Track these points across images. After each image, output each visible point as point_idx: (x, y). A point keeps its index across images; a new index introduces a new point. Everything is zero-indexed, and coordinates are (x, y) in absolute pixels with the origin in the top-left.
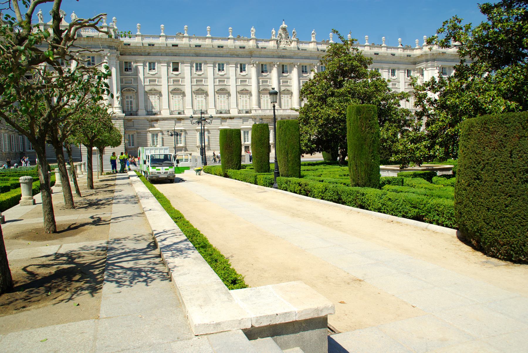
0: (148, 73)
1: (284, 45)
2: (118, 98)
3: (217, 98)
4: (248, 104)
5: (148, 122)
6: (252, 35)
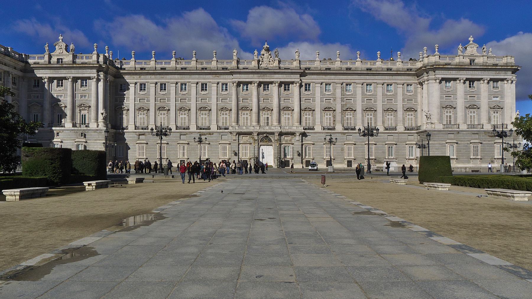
0: (139, 93)
1: (266, 65)
2: (102, 114)
3: (220, 115)
4: (228, 121)
5: (136, 135)
6: (234, 56)
